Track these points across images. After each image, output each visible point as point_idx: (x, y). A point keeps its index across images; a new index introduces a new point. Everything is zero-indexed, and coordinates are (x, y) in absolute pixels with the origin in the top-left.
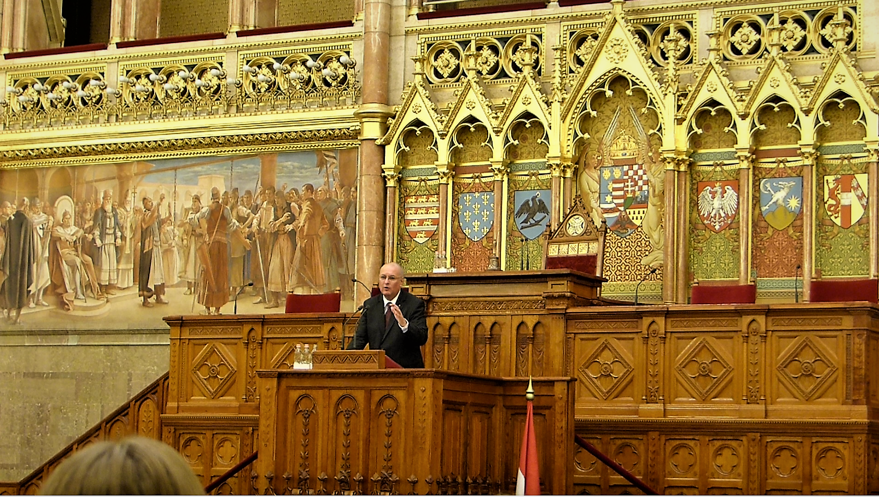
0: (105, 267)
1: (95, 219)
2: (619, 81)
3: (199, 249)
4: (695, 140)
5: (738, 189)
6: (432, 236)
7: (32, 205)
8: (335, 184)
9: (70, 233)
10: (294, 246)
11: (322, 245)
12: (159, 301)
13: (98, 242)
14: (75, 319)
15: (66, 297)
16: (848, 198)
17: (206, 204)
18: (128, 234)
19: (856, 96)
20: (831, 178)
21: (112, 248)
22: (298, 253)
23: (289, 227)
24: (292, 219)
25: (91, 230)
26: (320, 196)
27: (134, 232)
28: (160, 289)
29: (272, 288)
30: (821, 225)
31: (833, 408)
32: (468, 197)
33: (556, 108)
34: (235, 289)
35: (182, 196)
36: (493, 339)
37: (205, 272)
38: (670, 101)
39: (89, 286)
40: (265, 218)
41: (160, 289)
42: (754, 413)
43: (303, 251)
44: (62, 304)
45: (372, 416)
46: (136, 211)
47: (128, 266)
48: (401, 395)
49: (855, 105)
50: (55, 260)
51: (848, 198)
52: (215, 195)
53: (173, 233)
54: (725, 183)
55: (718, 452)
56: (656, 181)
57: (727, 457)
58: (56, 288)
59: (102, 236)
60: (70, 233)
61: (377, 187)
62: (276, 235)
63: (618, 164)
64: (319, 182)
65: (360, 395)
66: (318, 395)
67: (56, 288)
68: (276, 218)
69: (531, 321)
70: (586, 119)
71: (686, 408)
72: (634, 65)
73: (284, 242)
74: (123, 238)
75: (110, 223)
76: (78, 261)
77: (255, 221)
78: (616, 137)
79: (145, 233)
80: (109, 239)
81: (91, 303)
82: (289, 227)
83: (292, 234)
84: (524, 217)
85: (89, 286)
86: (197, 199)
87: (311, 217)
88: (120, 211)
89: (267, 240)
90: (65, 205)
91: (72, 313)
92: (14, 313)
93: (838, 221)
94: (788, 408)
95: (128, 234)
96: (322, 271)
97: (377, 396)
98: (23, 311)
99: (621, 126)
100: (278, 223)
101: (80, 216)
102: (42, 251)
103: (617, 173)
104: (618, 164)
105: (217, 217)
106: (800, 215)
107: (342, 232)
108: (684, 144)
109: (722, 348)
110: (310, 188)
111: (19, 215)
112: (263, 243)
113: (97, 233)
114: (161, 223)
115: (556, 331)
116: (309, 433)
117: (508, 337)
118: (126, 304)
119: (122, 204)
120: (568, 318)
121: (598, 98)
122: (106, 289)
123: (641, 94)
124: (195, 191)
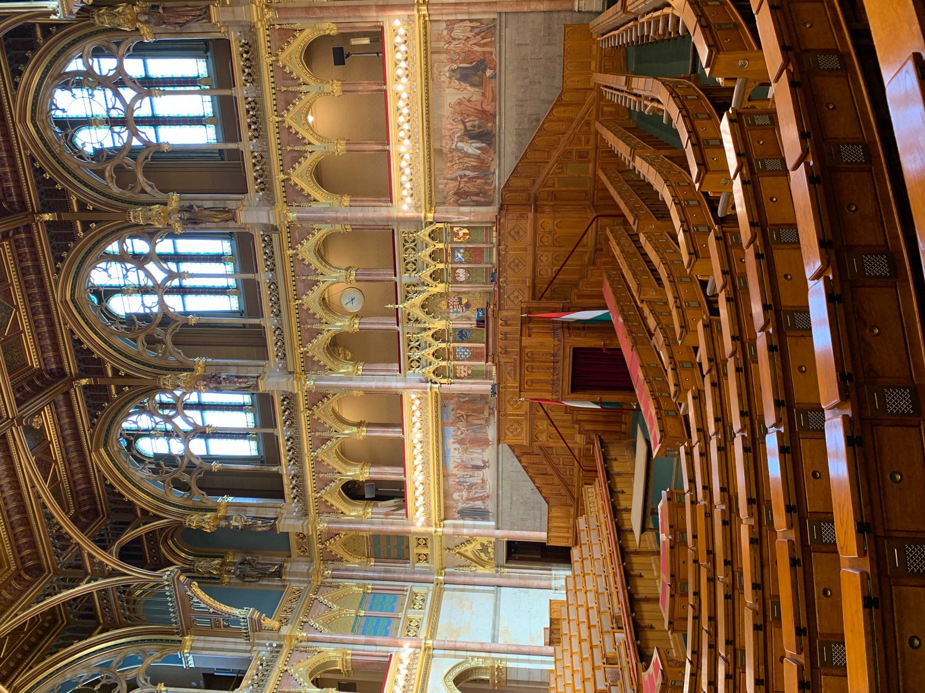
2: (423, 307)
4: (442, 282)
8: (452, 401)
11: (471, 406)
16: (461, 234)
17: (457, 446)
19: (430, 230)
28: (484, 462)
30: (469, 242)
31: (528, 225)
33: (431, 326)
35: (455, 454)
36: (506, 334)
38: (430, 289)
41: (484, 462)
42: (530, 249)
44: (488, 497)
45: (533, 361)
47: (476, 473)
48: (527, 351)
51: (461, 234)
52: (454, 443)
53: (466, 457)
54: (455, 273)
55: (541, 261)
57: (544, 259)
58: (482, 499)
60: (465, 494)
62: (467, 422)
63: (448, 307)
64: (451, 407)
65: (527, 364)
66: (526, 379)
67: (482, 499)
69: (500, 322)
71: (529, 273)
72: (418, 300)
73: (470, 419)
75: (462, 480)
79: (466, 467)
87: (462, 410)
90: (456, 496)
96: (480, 406)
97: (527, 358)
101: (459, 490)
102: (471, 504)
104: (448, 307)
105: (461, 442)
106: (465, 249)
108: (443, 285)
109: (510, 260)
115: (504, 313)
116: (539, 381)
117: (505, 329)
120: (500, 310)
121: (428, 313)
122: (483, 481)
123: (427, 299)
124: (452, 450)
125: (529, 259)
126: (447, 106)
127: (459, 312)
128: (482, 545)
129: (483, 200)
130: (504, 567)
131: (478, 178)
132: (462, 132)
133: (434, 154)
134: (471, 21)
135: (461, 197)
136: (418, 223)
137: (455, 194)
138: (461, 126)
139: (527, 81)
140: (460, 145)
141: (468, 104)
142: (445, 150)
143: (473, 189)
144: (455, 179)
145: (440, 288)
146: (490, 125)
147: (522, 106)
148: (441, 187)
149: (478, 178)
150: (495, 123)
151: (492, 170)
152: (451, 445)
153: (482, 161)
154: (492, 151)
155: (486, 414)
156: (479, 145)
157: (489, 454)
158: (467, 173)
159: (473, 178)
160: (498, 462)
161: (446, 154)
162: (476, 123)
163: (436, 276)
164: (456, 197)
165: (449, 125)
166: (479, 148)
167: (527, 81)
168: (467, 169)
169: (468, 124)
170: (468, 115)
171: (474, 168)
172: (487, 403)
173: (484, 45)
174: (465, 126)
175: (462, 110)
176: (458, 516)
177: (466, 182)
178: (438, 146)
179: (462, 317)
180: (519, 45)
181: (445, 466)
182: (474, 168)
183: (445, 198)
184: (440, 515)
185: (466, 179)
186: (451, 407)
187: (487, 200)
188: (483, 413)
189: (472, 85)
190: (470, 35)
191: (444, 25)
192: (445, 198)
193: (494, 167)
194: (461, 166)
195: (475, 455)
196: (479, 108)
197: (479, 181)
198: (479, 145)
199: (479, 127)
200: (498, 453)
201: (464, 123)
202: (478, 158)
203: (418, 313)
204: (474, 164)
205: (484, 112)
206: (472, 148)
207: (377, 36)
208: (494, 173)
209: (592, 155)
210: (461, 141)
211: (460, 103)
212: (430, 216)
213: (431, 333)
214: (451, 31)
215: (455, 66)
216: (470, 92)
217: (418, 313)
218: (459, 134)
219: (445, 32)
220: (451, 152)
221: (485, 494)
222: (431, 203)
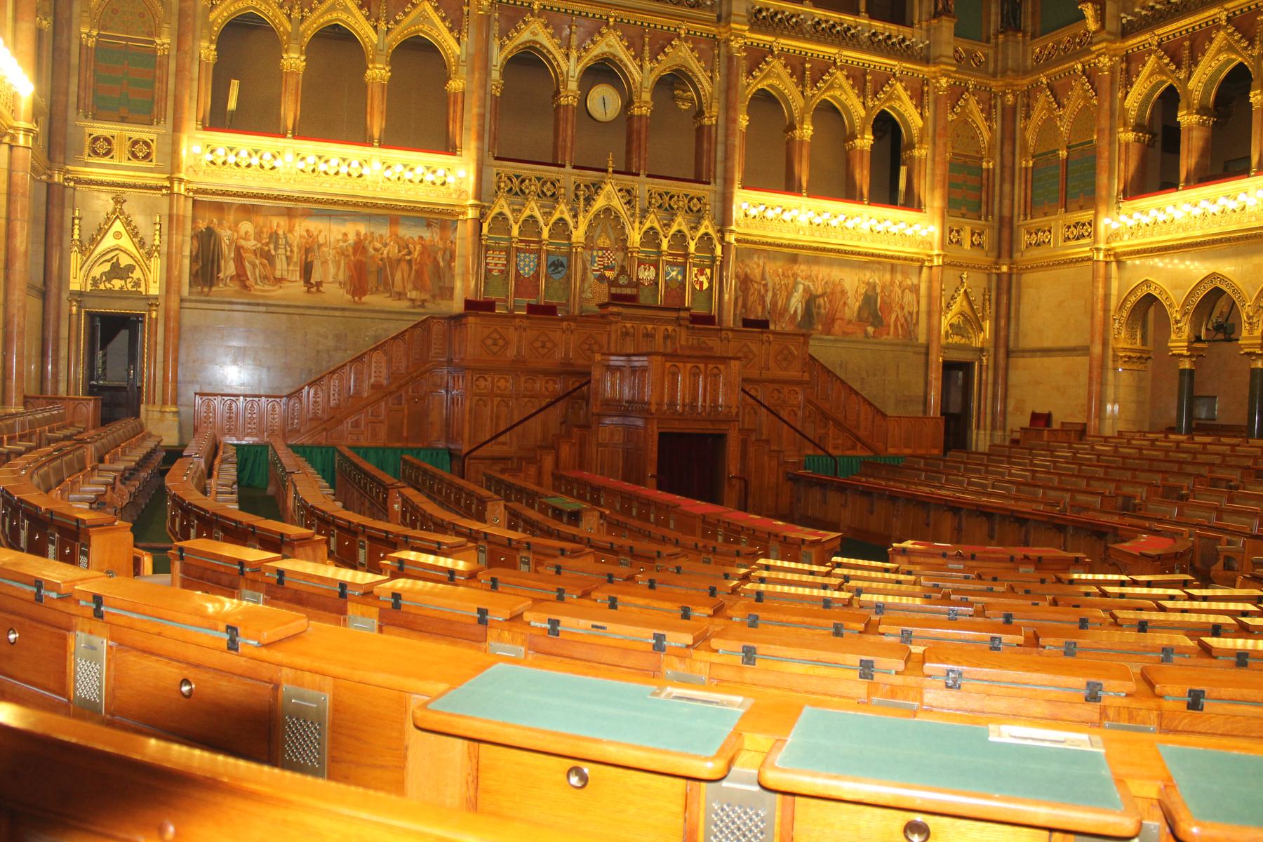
0: (278, 267)
1: (270, 237)
3: (347, 264)
5: (657, 268)
6: (501, 271)
7: (220, 224)
8: (437, 238)
9: (251, 244)
11: (428, 269)
12: (318, 291)
13: (273, 252)
14: (256, 297)
15: (248, 283)
16: (703, 278)
17: (352, 238)
18: (295, 250)
21: (284, 258)
22: (413, 272)
24: (410, 253)
25: (267, 244)
26: (428, 243)
27: (300, 250)
28: (319, 284)
29: (396, 289)
33: (581, 218)
35: (336, 234)
37: (351, 277)
39: (266, 278)
40: (392, 250)
43: (417, 271)
44: (246, 287)
46: (301, 237)
49: (710, 239)
50: (239, 259)
51: (703, 278)
52: (358, 234)
56: (619, 260)
58: (240, 276)
59: (276, 248)
60: (251, 244)
62: (399, 261)
63: (601, 249)
70: (590, 225)
73: (404, 266)
74: (292, 251)
76: (257, 262)
78: (600, 236)
79: (308, 250)
80: (281, 251)
81: (267, 288)
83: (409, 262)
85: (266, 278)
86: (345, 235)
87: (422, 254)
88: (289, 235)
89: (395, 263)
90: (246, 227)
91: (253, 292)
92: (206, 290)
95: (295, 250)
98: (214, 289)
101: (258, 236)
102: (228, 253)
103: (600, 253)
104: (601, 249)
105: (359, 247)
106: (683, 284)
107: (442, 264)
110: (421, 238)
111: (208, 229)
113: (272, 246)
114: (320, 246)
118: (295, 289)
119: (291, 230)
121: (597, 216)
123: (617, 218)
128: (130, 268)
130: (79, 307)
131: (764, 307)
133: (793, 254)
134: (918, 313)
135: (745, 282)
136: (724, 221)
137: (746, 275)
138: (820, 291)
139: (864, 375)
140: (801, 288)
142: (796, 267)
143: (751, 299)
144: (763, 278)
145: (635, 237)
146: (820, 327)
148: (756, 259)
149: (764, 307)
152: (353, 230)
153: (782, 315)
155: (414, 295)
156: (799, 311)
157: (335, 292)
158: (770, 294)
159: (764, 301)
160: (326, 308)
162: (823, 311)
163: (651, 237)
164: (742, 277)
165: (824, 274)
166: (796, 311)
167: (864, 375)
168: (774, 295)
169: (821, 300)
170: (830, 301)
171: (774, 303)
172: (434, 297)
173: (896, 326)
175: (835, 293)
176: (202, 225)
180: (898, 366)
181: (308, 214)
182: (774, 303)
183: (742, 261)
184: (204, 192)
186: (427, 235)
188: (415, 288)
189: (860, 308)
190: (906, 311)
191: (915, 281)
192: (742, 261)
195: (332, 269)
196: (838, 315)
197: (760, 309)
198: (799, 311)
199: (818, 314)
200: (343, 309)
202: (786, 309)
205: (833, 321)
206: (796, 303)
207: (912, 202)
210: (804, 290)
211: (843, 292)
212: (731, 238)
213: (567, 217)
214: (911, 291)
215: (878, 290)
216: (854, 305)
217: (600, 203)
219: (909, 282)
221: (251, 281)
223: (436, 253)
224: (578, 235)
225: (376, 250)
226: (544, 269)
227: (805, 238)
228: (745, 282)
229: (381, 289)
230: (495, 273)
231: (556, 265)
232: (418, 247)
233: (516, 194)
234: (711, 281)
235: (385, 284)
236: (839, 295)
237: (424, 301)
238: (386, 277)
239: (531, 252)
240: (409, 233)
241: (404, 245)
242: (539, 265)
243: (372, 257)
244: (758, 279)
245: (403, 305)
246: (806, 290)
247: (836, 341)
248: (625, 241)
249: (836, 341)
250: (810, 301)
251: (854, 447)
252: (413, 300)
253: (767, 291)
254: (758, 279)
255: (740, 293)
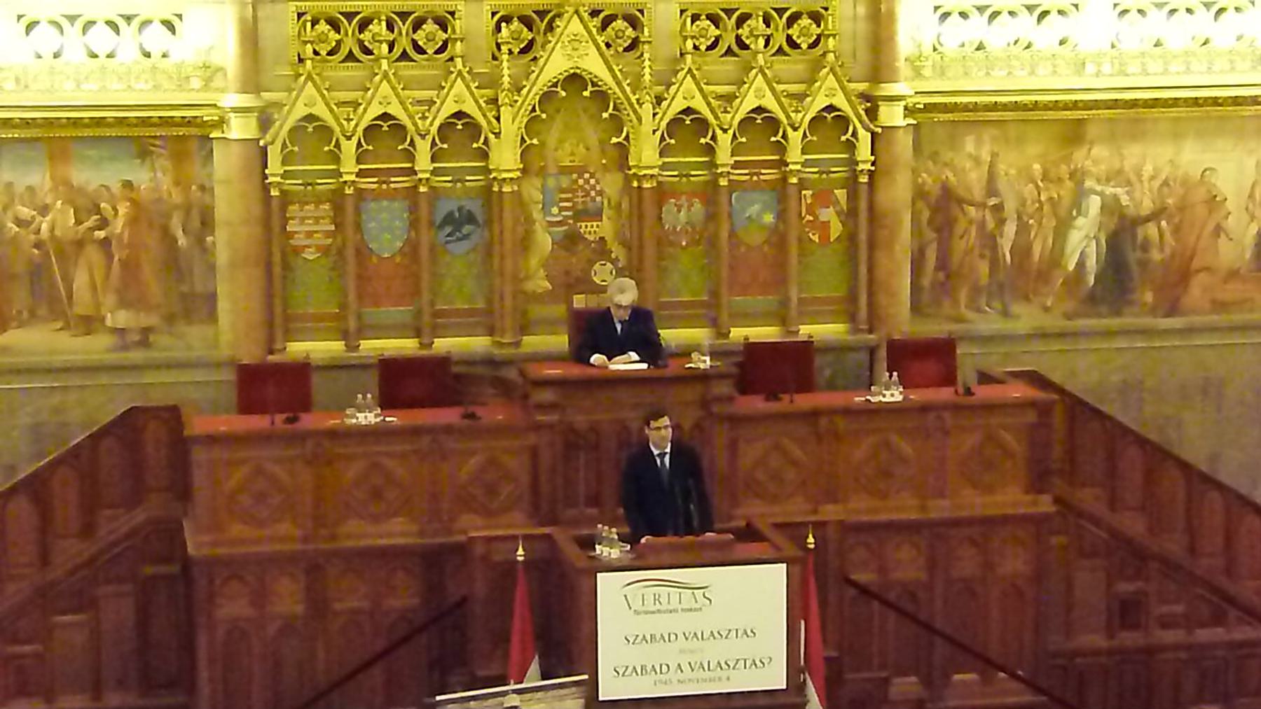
6: (325, 251)
8: (166, 182)
10: (110, 257)
20: (808, 193)
23: (101, 234)
24: (104, 223)
29: (79, 310)
31: (1011, 498)
32: (373, 205)
33: (506, 113)
34: (20, 312)
42: (940, 509)
43: (124, 264)
49: (843, 121)
61: (257, 194)
62: (80, 244)
63: (565, 171)
68: (79, 222)
70: (532, 124)
73: (93, 254)
77: (44, 227)
78: (561, 141)
82: (101, 234)
83: (106, 243)
84: (448, 229)
87: (133, 221)
93: (816, 238)
94: (974, 503)
99: (566, 126)
100: (82, 228)
103: (565, 182)
107: (182, 241)
110: (128, 185)
112: (61, 255)
121: (547, 97)
123: (601, 97)
125: (904, 508)
126: (1208, 159)
127: (545, 209)
129: (926, 282)
131: (995, 263)
132: (1131, 211)
133: (1070, 122)
138: (1147, 206)
140: (1094, 203)
141: (1211, 226)
142: (1080, 157)
143: (959, 246)
144: (992, 190)
146: (1149, 297)
147: (1205, 392)
148: (969, 145)
149: (995, 263)
150: (1153, 311)
151: (1016, 308)
153: (1044, 276)
154: (1070, 305)
155: (121, 318)
156: (1092, 264)
158: (1010, 229)
161: (1067, 159)
162: (1156, 255)
165: (1157, 162)
166: (1081, 264)
168: (1023, 228)
169: (1151, 230)
170: (1177, 230)
171: (1022, 251)
172: (170, 319)
174: (1147, 219)
175: (1192, 207)
177: (982, 225)
178: (1092, 131)
179: (530, 221)
182: (1022, 251)
185: (991, 224)
186: (142, 176)
187: (926, 297)
188: (124, 303)
192: (934, 156)
193: (1026, 318)
194: (1031, 208)
197: (984, 268)
199: (1144, 264)
201: (1155, 216)
202: (1055, 258)
203: (555, 64)
204: (1037, 250)
206: (1083, 242)
208: (1006, 314)
209: (1129, 639)
211: (1214, 202)
212: (892, 116)
218: (1125, 200)
220: (1072, 175)
222: (929, 108)
223: (168, 216)
224: (505, 158)
225: (19, 222)
226: (425, 237)
227: (1100, 81)
228: (942, 207)
229: (42, 311)
230: (310, 255)
231: (458, 221)
232: (122, 210)
233: (350, 57)
234: (850, 215)
235: (48, 300)
236: (1201, 211)
237: (146, 331)
238: (53, 285)
239: (393, 195)
240: (100, 175)
241: (88, 206)
242: (414, 224)
243: (15, 240)
244: (978, 193)
245: (96, 347)
246: (1110, 207)
247: (1190, 331)
248: (623, 149)
249: (1190, 331)
250: (1121, 234)
251: (1218, 619)
252: (121, 332)
253: (1001, 222)
254: (978, 193)
255: (930, 235)
